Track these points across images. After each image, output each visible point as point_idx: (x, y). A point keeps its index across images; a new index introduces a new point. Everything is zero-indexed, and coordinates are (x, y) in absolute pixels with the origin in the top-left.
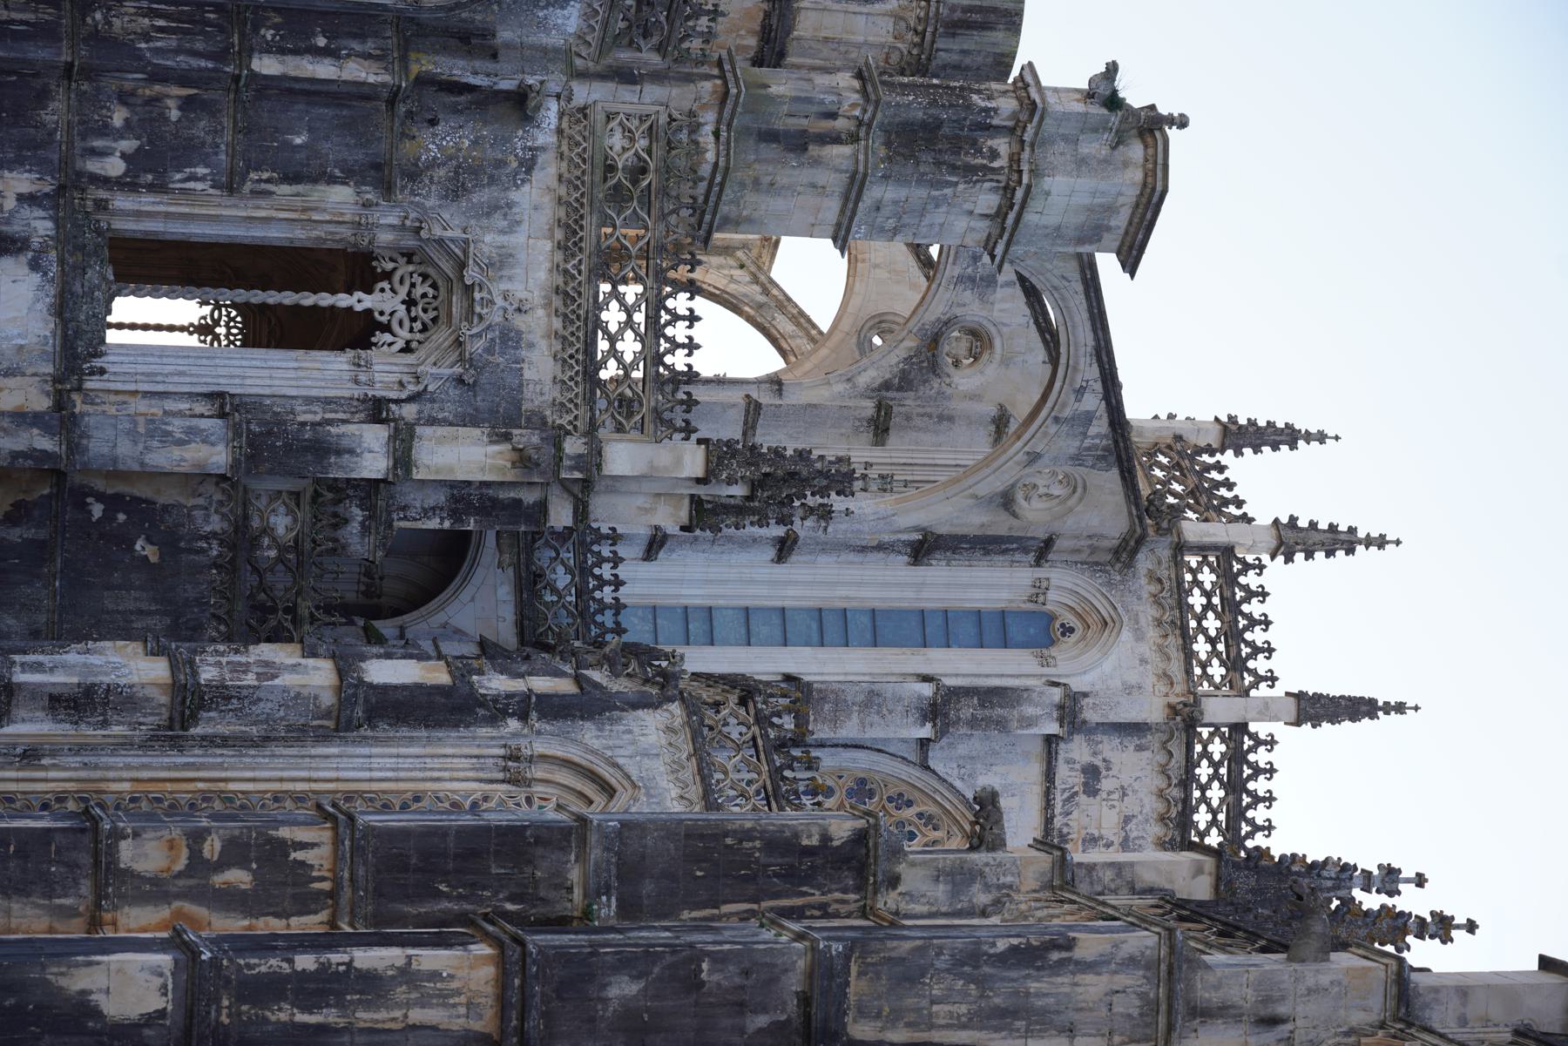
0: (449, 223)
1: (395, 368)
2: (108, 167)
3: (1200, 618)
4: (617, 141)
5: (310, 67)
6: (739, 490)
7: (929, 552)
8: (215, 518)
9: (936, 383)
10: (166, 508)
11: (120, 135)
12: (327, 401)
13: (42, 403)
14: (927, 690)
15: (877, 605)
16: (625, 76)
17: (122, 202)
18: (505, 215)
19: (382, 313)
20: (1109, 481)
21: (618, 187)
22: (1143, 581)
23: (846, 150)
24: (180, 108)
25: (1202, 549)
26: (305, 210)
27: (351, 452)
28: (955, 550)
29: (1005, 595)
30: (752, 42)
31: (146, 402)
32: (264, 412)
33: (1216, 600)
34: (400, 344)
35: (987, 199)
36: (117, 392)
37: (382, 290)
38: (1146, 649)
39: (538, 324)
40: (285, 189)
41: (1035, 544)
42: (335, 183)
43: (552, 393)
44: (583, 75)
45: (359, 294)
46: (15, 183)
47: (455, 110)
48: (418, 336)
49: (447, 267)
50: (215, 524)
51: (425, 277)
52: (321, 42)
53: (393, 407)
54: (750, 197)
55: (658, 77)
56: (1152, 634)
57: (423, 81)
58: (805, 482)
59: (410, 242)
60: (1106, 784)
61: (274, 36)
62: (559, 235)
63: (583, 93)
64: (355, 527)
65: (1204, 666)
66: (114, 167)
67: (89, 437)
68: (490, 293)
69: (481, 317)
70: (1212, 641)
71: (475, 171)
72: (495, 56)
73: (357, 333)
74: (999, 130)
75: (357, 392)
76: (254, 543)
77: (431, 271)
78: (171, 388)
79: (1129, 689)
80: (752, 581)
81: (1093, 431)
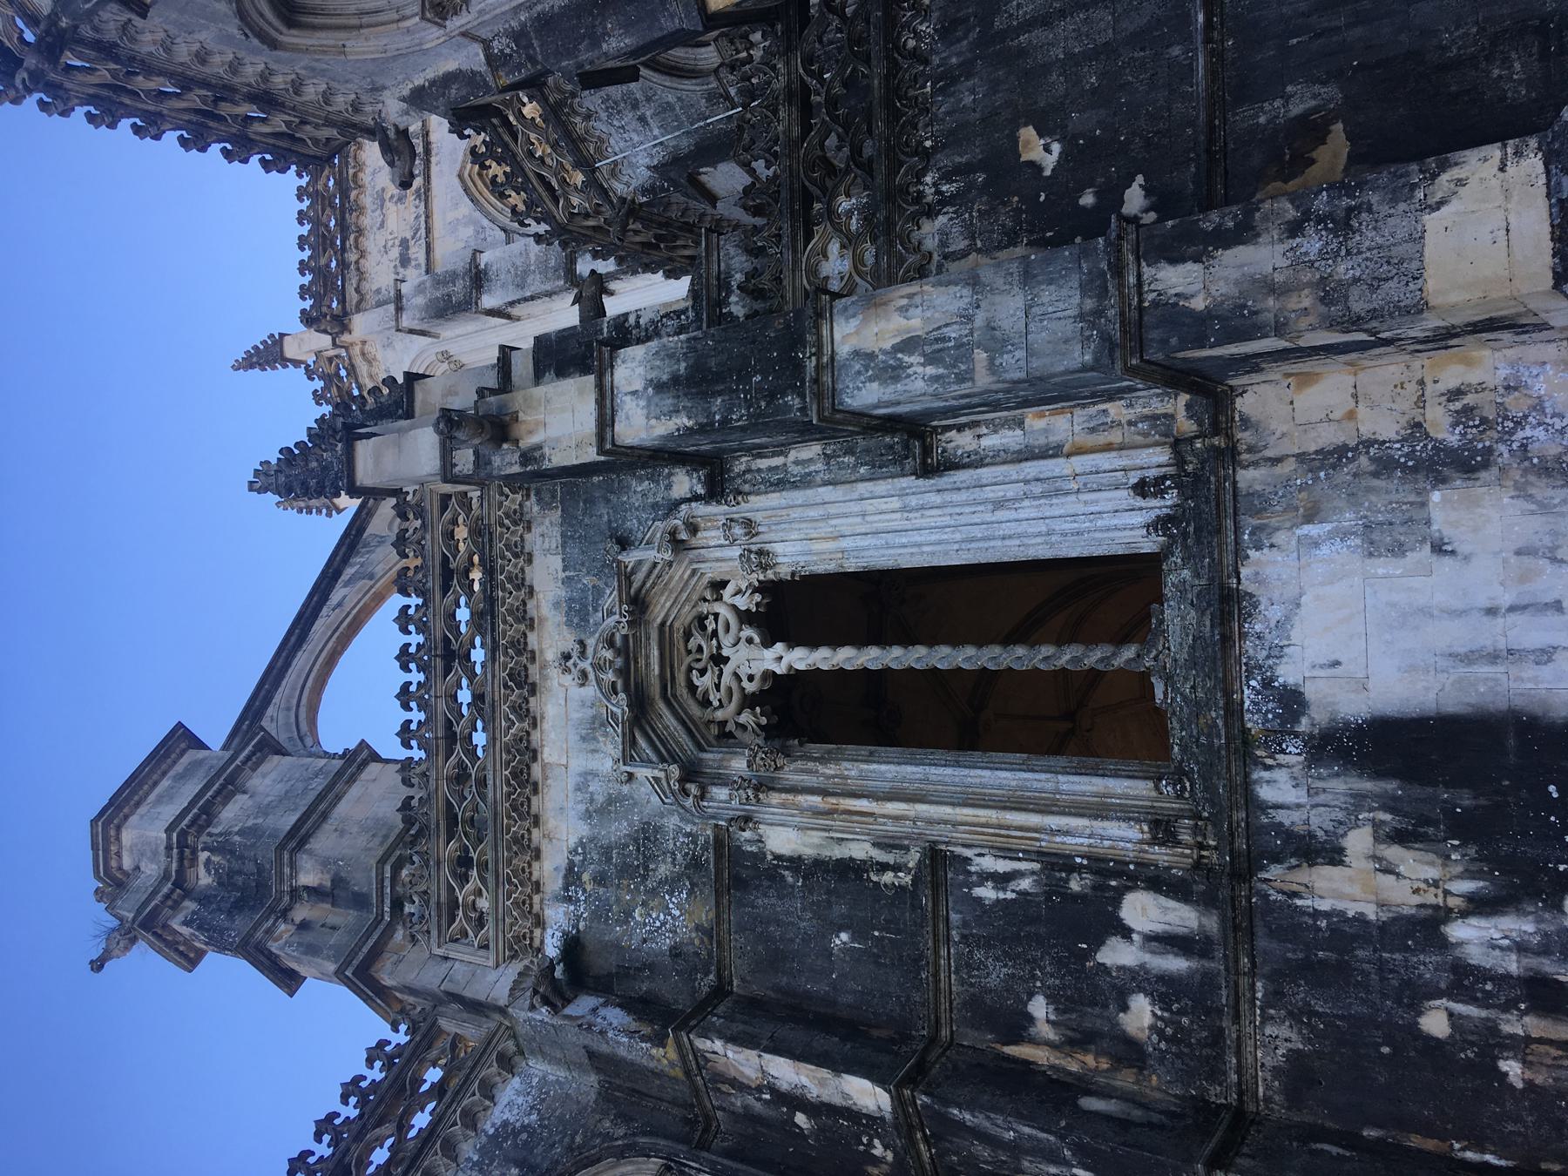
1: (718, 554)
2: (1154, 913)
5: (804, 1080)
8: (930, 244)
11: (1138, 979)
12: (781, 484)
13: (1261, 400)
17: (1124, 837)
18: (592, 801)
19: (750, 641)
24: (1031, 1019)
27: (660, 387)
32: (867, 451)
34: (727, 593)
35: (232, 814)
36: (1108, 448)
37: (751, 678)
40: (860, 850)
42: (791, 859)
45: (780, 669)
46: (1356, 890)
47: (651, 967)
48: (704, 608)
51: (705, 703)
52: (801, 1119)
53: (700, 490)
60: (395, 253)
61: (870, 1145)
66: (1144, 911)
67: (1081, 317)
68: (599, 681)
69: (610, 643)
71: (626, 871)
73: (790, 607)
77: (695, 710)
78: (1012, 471)
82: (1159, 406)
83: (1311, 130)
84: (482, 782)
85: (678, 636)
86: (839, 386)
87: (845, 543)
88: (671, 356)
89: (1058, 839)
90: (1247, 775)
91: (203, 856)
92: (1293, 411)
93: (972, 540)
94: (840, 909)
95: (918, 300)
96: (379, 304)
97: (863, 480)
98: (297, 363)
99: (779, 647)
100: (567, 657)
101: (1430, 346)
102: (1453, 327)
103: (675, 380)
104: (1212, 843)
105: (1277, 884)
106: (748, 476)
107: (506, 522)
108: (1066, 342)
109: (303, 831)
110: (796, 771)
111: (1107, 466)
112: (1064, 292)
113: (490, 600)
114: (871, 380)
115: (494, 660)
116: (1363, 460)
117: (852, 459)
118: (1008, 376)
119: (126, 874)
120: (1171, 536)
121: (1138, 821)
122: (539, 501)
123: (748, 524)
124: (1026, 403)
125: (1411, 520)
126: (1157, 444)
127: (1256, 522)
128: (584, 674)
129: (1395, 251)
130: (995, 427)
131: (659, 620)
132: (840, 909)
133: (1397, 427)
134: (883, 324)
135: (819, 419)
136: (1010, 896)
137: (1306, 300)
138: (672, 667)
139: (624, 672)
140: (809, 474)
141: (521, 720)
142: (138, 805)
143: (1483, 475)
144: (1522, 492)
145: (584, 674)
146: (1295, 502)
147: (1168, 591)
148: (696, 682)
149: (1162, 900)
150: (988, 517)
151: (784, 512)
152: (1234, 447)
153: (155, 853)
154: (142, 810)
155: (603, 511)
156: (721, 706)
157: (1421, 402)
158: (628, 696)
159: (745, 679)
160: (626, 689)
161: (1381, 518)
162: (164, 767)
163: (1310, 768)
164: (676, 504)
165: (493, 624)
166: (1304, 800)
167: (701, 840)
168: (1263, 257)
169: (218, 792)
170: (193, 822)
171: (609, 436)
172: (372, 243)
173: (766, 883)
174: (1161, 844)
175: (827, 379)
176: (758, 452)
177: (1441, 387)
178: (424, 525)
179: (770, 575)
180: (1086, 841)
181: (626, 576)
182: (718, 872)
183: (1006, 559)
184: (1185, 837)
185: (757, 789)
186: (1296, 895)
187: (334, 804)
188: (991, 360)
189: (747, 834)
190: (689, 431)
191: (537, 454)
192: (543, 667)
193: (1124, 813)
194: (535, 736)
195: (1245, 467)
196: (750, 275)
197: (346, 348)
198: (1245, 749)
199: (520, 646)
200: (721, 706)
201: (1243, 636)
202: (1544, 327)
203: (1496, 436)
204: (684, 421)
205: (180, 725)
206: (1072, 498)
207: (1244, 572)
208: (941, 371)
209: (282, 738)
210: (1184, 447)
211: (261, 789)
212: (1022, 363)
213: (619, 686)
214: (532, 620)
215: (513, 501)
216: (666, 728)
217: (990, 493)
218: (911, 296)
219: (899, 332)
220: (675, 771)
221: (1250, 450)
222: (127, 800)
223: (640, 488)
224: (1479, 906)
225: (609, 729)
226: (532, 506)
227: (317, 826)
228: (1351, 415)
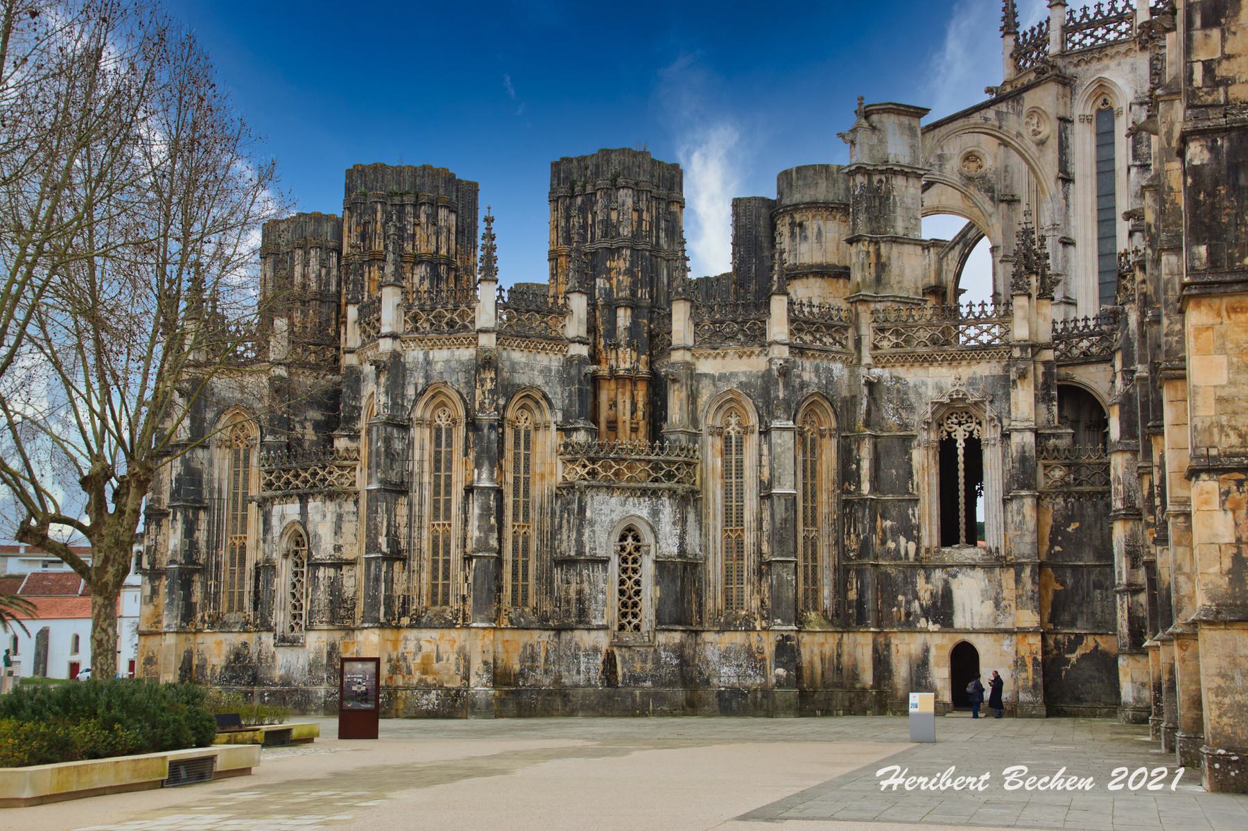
0: (924, 411)
3: (1097, 39)
4: (885, 343)
6: (1033, 279)
7: (1068, 174)
9: (989, 176)
10: (1054, 521)
11: (898, 544)
12: (1004, 456)
14: (1134, 171)
15: (1095, 194)
16: (858, 343)
17: (925, 543)
20: (1030, 99)
21: (904, 341)
22: (1079, 69)
23: (882, 245)
25: (1064, 42)
28: (1066, 162)
29: (1088, 135)
30: (841, 281)
33: (1088, 31)
38: (1113, 64)
39: (966, 371)
40: (915, 478)
41: (1062, 125)
43: (994, 363)
44: (860, 360)
49: (943, 410)
50: (1060, 500)
54: (906, 284)
55: (857, 329)
56: (1106, 61)
57: (867, 424)
58: (1028, 249)
59: (934, 425)
62: (926, 364)
63: (867, 358)
64: (1058, 442)
65: (1121, 34)
66: (912, 547)
70: (1109, 31)
71: (902, 401)
72: (854, 397)
73: (974, 446)
74: (870, 181)
75: (999, 445)
76: (1068, 484)
79: (1134, 69)
80: (1085, 254)
81: (1005, 110)
83: (1063, 583)
94: (901, 472)
168: (1029, 586)
193: (931, 541)
224: (921, 605)
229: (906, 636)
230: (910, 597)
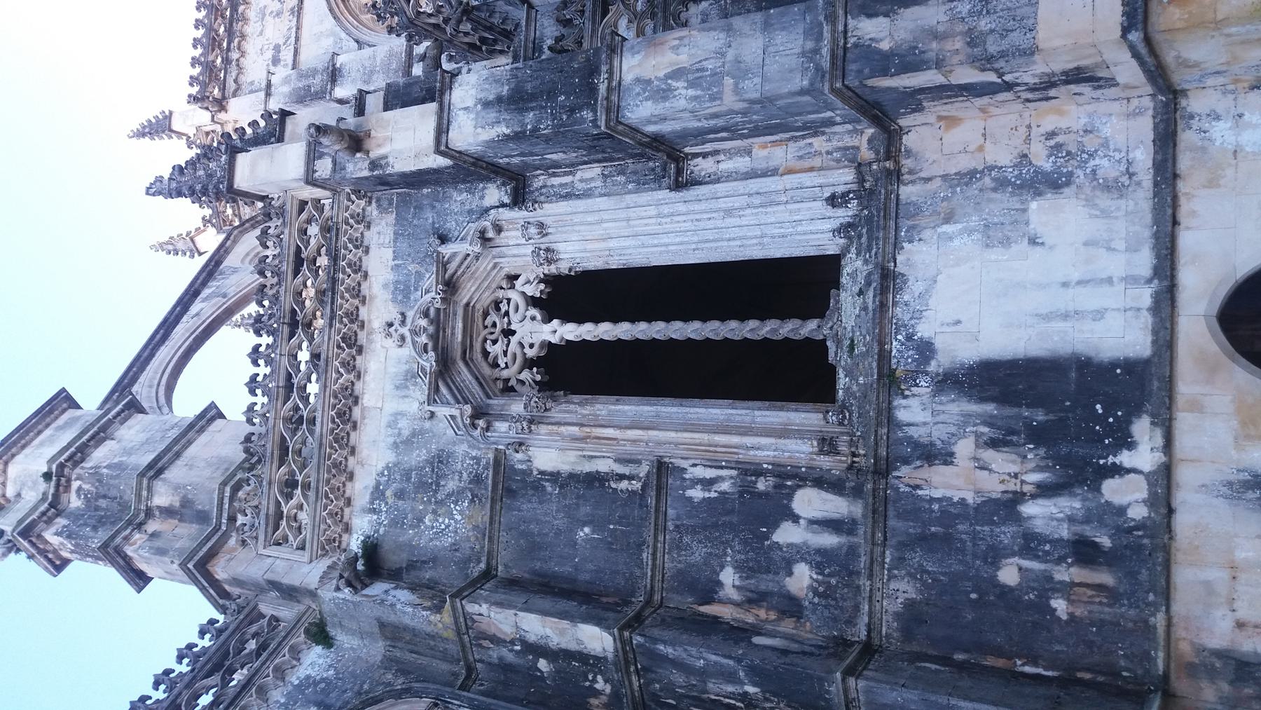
1: (515, 251)
5: (549, 632)
11: (800, 553)
12: (568, 196)
17: (800, 451)
18: (399, 434)
19: (533, 318)
24: (720, 584)
26: (583, 439)
27: (487, 104)
31: (772, 164)
32: (635, 173)
34: (518, 283)
35: (101, 455)
36: (811, 169)
40: (604, 466)
42: (552, 474)
43: (371, 237)
45: (555, 339)
46: (960, 482)
48: (501, 294)
51: (495, 365)
52: (543, 664)
53: (507, 200)
60: (269, 54)
61: (594, 681)
66: (809, 502)
67: (803, 54)
68: (414, 343)
69: (426, 314)
71: (422, 486)
77: (487, 370)
82: (849, 141)
84: (312, 421)
85: (478, 315)
86: (623, 104)
87: (612, 244)
88: (496, 81)
89: (752, 453)
90: (890, 403)
91: (75, 485)
92: (941, 143)
93: (707, 241)
94: (585, 510)
95: (686, 41)
96: (251, 92)
97: (630, 192)
98: (180, 135)
99: (555, 322)
100: (390, 325)
101: (1037, 95)
102: (1053, 74)
103: (499, 100)
104: (862, 452)
105: (906, 480)
106: (544, 191)
107: (351, 221)
108: (791, 71)
109: (160, 465)
110: (560, 412)
111: (808, 184)
112: (792, 37)
113: (334, 281)
114: (647, 99)
115: (331, 326)
116: (987, 180)
117: (623, 178)
118: (747, 96)
119: (8, 501)
120: (850, 238)
121: (810, 439)
122: (379, 206)
123: (541, 226)
124: (756, 132)
125: (1016, 221)
126: (846, 167)
127: (910, 223)
128: (403, 338)
129: (1018, 12)
130: (731, 154)
131: (465, 301)
132: (585, 510)
133: (1011, 157)
134: (659, 59)
135: (607, 127)
136: (713, 495)
137: (958, 44)
138: (471, 337)
139: (435, 338)
140: (590, 189)
141: (348, 372)
142: (23, 447)
143: (1066, 190)
144: (1090, 203)
145: (403, 338)
146: (939, 209)
147: (844, 280)
148: (489, 349)
149: (824, 495)
150: (719, 223)
151: (569, 218)
152: (899, 171)
153: (35, 483)
154: (27, 451)
155: (429, 216)
156: (507, 367)
157: (1028, 140)
158: (437, 355)
159: (527, 346)
160: (435, 349)
161: (996, 220)
162: (48, 420)
163: (934, 396)
164: (487, 210)
165: (333, 298)
166: (929, 419)
167: (484, 462)
169: (92, 438)
170: (70, 458)
171: (444, 141)
172: (251, 46)
173: (531, 492)
174: (828, 454)
175: (614, 98)
176: (552, 168)
177: (1042, 130)
178: (284, 223)
179: (553, 269)
180: (772, 453)
181: (443, 264)
182: (495, 484)
183: (729, 259)
184: (843, 448)
185: (531, 422)
186: (918, 487)
187: (186, 447)
188: (736, 85)
189: (519, 456)
190: (507, 138)
191: (383, 162)
192: (369, 334)
193: (800, 434)
194: (358, 386)
195: (906, 184)
196: (558, 40)
197: (222, 125)
198: (890, 382)
199: (353, 316)
200: (507, 367)
201: (895, 304)
202: (1111, 82)
203: (1076, 164)
204: (504, 130)
205: (63, 390)
206: (781, 208)
207: (899, 258)
208: (699, 92)
209: (145, 405)
210: (863, 169)
211: (126, 437)
212: (759, 87)
213: (430, 347)
214: (364, 297)
215: (358, 206)
216: (463, 381)
217: (722, 204)
218: (681, 39)
219: (671, 64)
220: (468, 409)
221: (911, 172)
222: (15, 443)
223: (459, 199)
224: (1044, 491)
225: (419, 380)
226: (373, 210)
227: (171, 462)
228: (981, 149)
229: (1185, 576)
230: (1007, 534)
